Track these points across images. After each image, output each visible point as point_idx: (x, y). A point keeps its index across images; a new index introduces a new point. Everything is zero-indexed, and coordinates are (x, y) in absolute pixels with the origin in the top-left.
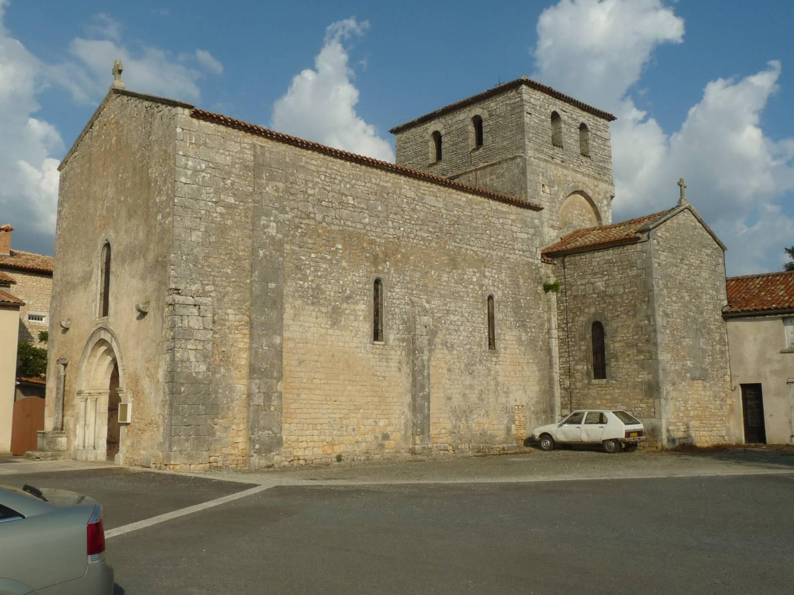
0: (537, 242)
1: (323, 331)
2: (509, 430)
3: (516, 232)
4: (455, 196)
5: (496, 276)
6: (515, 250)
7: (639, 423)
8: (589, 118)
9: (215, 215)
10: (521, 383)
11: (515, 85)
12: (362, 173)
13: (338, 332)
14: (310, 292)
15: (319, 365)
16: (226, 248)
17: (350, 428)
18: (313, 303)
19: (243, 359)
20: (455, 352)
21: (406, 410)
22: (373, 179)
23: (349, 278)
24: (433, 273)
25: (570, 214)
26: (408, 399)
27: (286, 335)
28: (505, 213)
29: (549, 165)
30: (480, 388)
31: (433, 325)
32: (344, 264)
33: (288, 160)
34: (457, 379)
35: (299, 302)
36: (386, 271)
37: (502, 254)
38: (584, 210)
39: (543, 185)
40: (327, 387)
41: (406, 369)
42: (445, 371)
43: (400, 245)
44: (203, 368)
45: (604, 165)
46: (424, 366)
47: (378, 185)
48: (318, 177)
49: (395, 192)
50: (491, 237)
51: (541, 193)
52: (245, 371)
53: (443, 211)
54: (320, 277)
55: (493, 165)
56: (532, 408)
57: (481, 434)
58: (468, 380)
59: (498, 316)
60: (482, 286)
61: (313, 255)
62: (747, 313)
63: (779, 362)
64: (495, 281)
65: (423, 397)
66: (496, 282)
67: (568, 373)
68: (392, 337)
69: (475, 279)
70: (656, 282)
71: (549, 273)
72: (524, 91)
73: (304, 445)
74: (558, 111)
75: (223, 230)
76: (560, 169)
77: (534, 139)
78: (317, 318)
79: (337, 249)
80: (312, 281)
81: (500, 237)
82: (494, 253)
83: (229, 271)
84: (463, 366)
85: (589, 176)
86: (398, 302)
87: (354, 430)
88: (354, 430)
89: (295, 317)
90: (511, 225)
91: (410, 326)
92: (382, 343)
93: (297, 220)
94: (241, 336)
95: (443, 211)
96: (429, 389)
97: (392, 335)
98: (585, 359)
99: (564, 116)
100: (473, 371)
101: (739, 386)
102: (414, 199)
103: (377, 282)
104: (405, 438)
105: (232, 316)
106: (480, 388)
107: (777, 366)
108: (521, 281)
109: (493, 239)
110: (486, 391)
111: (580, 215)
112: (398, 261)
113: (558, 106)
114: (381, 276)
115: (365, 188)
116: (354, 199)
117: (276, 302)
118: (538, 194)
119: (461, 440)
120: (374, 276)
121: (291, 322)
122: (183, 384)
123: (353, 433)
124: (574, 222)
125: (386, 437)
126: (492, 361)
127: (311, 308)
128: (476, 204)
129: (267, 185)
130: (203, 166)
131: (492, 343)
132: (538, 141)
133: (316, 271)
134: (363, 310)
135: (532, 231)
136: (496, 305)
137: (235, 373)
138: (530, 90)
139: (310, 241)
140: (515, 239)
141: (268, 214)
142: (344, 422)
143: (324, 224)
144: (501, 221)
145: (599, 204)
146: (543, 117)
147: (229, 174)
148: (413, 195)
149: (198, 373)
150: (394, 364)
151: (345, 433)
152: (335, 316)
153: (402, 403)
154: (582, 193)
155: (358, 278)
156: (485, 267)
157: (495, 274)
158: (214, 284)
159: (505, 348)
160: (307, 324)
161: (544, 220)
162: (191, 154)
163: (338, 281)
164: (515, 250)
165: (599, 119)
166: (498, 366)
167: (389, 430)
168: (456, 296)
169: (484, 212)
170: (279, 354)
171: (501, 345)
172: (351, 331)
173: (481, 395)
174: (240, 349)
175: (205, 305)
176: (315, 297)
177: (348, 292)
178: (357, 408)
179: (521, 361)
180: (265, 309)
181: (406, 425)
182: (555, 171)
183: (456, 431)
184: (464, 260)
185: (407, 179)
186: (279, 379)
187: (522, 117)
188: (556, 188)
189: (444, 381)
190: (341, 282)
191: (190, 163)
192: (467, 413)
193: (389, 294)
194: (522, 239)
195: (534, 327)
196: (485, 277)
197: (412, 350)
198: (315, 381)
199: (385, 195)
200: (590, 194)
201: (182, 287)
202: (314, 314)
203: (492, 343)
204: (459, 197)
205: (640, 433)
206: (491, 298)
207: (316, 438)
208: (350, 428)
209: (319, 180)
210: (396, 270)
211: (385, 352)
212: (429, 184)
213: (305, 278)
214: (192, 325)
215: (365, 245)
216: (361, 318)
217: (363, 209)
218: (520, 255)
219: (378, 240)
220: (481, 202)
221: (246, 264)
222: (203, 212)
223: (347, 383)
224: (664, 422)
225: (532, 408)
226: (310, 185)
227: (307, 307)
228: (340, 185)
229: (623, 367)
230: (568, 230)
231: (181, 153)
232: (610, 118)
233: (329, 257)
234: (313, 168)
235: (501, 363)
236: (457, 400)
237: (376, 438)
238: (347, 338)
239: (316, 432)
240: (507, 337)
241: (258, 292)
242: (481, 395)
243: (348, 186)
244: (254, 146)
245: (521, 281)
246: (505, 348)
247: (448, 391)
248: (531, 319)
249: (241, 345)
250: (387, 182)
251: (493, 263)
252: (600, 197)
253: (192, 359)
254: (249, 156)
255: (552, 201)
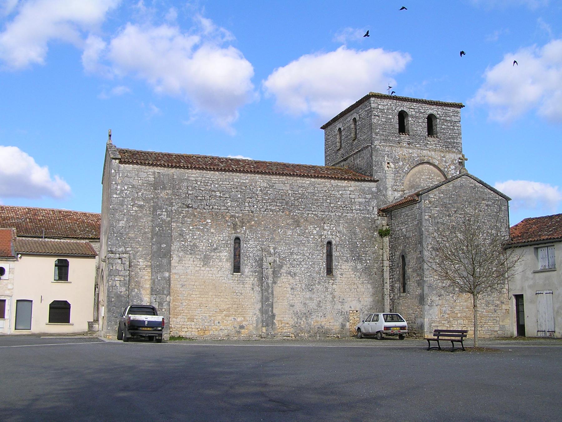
0: (374, 203)
1: (198, 268)
2: (343, 326)
3: (354, 199)
4: (301, 181)
5: (334, 229)
6: (353, 210)
7: (404, 321)
8: (438, 109)
9: (132, 212)
10: (356, 296)
11: (367, 98)
12: (227, 177)
13: (208, 269)
14: (189, 248)
15: (195, 287)
16: (138, 228)
17: (216, 322)
18: (191, 254)
19: (148, 285)
20: (297, 278)
21: (258, 313)
22: (235, 180)
23: (216, 238)
24: (279, 230)
25: (417, 180)
26: (259, 306)
27: (173, 271)
28: (345, 187)
29: (394, 149)
30: (318, 299)
31: (279, 262)
32: (212, 230)
33: (175, 177)
34: (298, 294)
35: (181, 254)
36: (243, 232)
37: (340, 214)
38: (432, 175)
39: (388, 163)
40: (201, 299)
41: (258, 289)
42: (289, 290)
43: (254, 216)
44: (123, 289)
45: (452, 141)
46: (268, 286)
47: (238, 182)
48: (196, 183)
49: (251, 185)
50: (330, 203)
51: (386, 169)
52: (149, 291)
53: (290, 192)
54: (195, 239)
55: (359, 151)
56: (366, 312)
57: (318, 328)
58: (308, 295)
59: (335, 254)
60: (322, 235)
61: (191, 227)
62: (542, 242)
63: (532, 279)
64: (334, 232)
65: (268, 305)
66: (333, 232)
67: (392, 289)
68: (247, 270)
69: (315, 232)
70: (426, 229)
71: (383, 222)
72: (372, 102)
73: (186, 330)
74: (405, 109)
75: (136, 219)
76: (405, 149)
77: (381, 132)
78: (194, 261)
79: (207, 223)
80: (190, 241)
81: (339, 203)
82: (334, 214)
83: (140, 240)
84: (304, 286)
85: (435, 150)
86: (251, 250)
87: (219, 322)
88: (219, 322)
89: (180, 261)
90: (350, 194)
91: (260, 263)
92: (240, 274)
93: (180, 209)
94: (146, 273)
95: (290, 192)
96: (273, 300)
97: (247, 269)
98: (398, 280)
99: (411, 112)
100: (313, 289)
101: (513, 297)
102: (266, 188)
103: (237, 239)
104: (257, 328)
105: (142, 263)
106: (318, 299)
107: (531, 282)
108: (358, 230)
109: (332, 205)
110: (324, 302)
111: (429, 178)
112: (253, 226)
113: (405, 107)
114: (239, 235)
115: (230, 185)
116: (220, 193)
117: (167, 254)
118: (383, 170)
119: (301, 331)
120: (234, 236)
121: (177, 264)
122: (113, 297)
123: (218, 325)
124: (422, 185)
125: (242, 327)
126: (329, 282)
127: (190, 256)
128: (318, 184)
129: (161, 193)
130: (126, 188)
131: (329, 271)
132: (385, 133)
133: (193, 236)
134: (225, 256)
135: (369, 196)
136: (334, 247)
137: (143, 292)
138: (379, 100)
139: (189, 220)
140: (352, 203)
141: (161, 208)
142: (212, 318)
143: (198, 210)
144: (340, 192)
145: (446, 169)
146: (391, 116)
147: (140, 190)
148: (265, 185)
149: (121, 292)
150: (248, 286)
151: (213, 324)
152: (206, 260)
153: (255, 308)
154: (428, 163)
155: (224, 236)
156: (324, 223)
157: (333, 227)
158: (131, 247)
159: (342, 274)
160: (187, 265)
161: (388, 186)
162: (120, 182)
163: (208, 240)
164: (353, 210)
165: (449, 108)
166: (334, 286)
167: (244, 323)
168: (298, 244)
169: (325, 189)
170: (169, 280)
171: (338, 272)
172: (217, 268)
173: (319, 304)
174: (146, 280)
175: (125, 258)
176: (193, 250)
177: (215, 246)
178: (221, 311)
179: (356, 282)
180: (161, 257)
181: (257, 321)
182: (402, 151)
183: (297, 325)
184: (307, 220)
185: (260, 176)
186: (169, 294)
187: (371, 119)
188: (401, 163)
189: (288, 295)
190: (210, 241)
191: (119, 187)
192: (307, 315)
193: (245, 245)
194: (359, 202)
195: (369, 260)
196: (325, 230)
197: (261, 278)
198: (192, 296)
199: (243, 188)
200: (437, 163)
201: (114, 250)
202: (192, 259)
203: (329, 271)
204: (304, 182)
205: (403, 328)
206: (329, 243)
207: (193, 327)
208: (216, 322)
209: (196, 185)
210: (250, 231)
211: (241, 279)
212: (278, 177)
213: (185, 240)
214: (117, 268)
215: (227, 219)
216: (224, 260)
217: (226, 198)
218: (357, 213)
219: (237, 215)
220: (323, 182)
221: (149, 235)
222: (125, 211)
223: (214, 297)
224: (426, 320)
225: (366, 312)
226: (191, 189)
227: (187, 256)
228: (211, 186)
229: (411, 284)
230: (415, 190)
231: (114, 183)
232: (460, 106)
233: (202, 228)
234: (193, 179)
235: (337, 284)
236: (299, 307)
237: (235, 328)
238: (214, 272)
239: (193, 323)
240: (343, 267)
241: (155, 250)
242: (319, 304)
243: (217, 186)
244: (154, 173)
245: (358, 230)
246: (342, 274)
247: (291, 301)
248: (366, 254)
249: (147, 277)
250: (246, 179)
251: (332, 220)
252: (447, 164)
253: (118, 285)
254: (151, 179)
255: (396, 172)
